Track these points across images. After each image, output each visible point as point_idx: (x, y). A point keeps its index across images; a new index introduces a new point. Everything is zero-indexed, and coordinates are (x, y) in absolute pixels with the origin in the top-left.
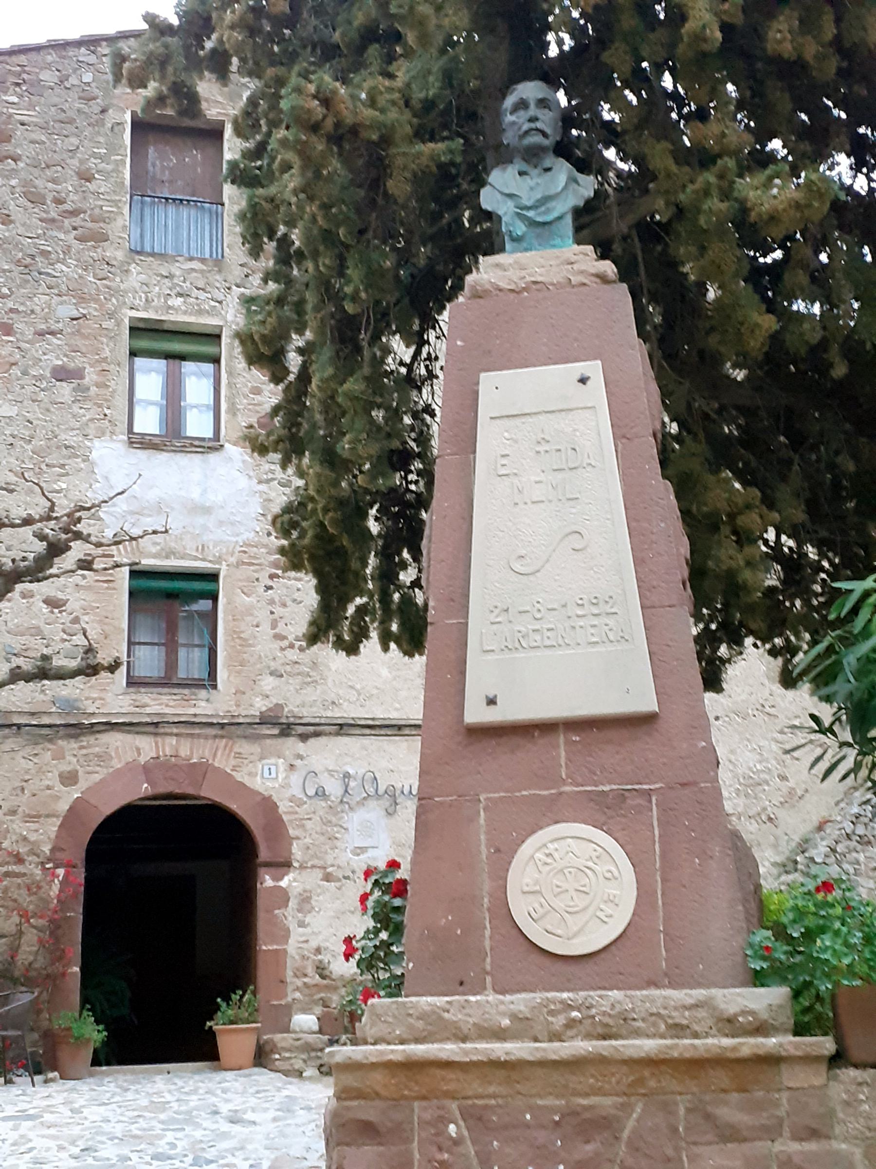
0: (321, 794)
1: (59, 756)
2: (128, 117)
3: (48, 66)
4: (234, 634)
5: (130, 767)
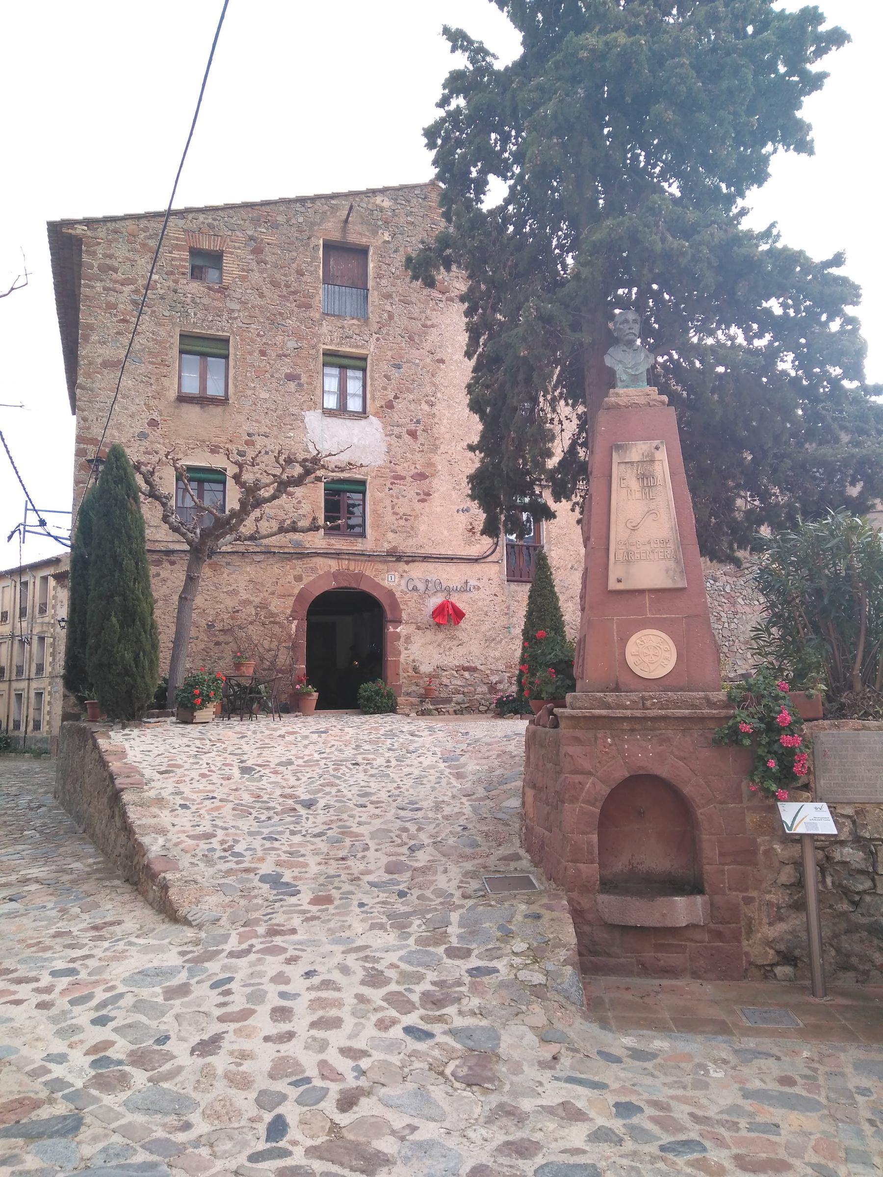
0: (415, 589)
2: (321, 242)
3: (281, 213)
4: (375, 511)
5: (327, 573)
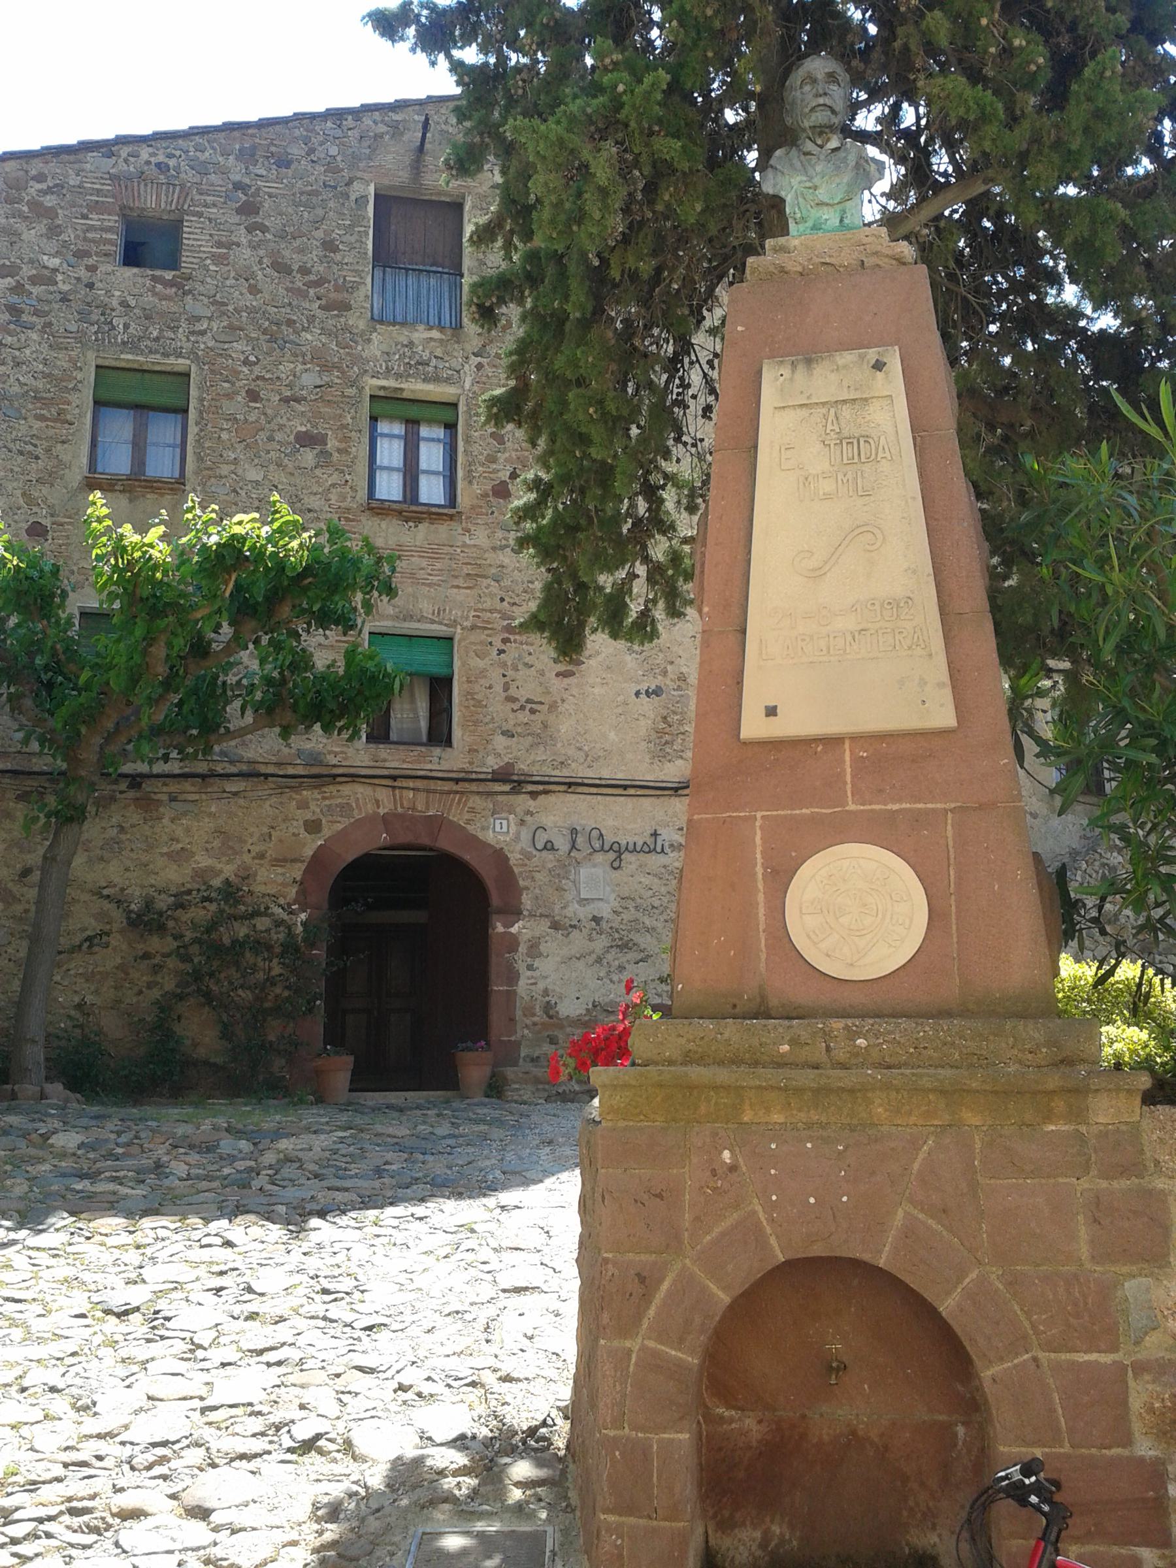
0: (549, 847)
1: (303, 805)
2: (371, 189)
5: (372, 819)
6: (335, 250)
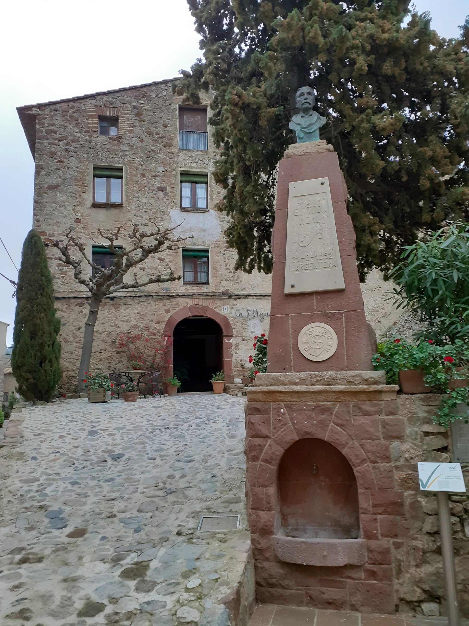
0: (241, 315)
1: (165, 305)
2: (178, 106)
3: (152, 91)
4: (214, 268)
6: (167, 127)
